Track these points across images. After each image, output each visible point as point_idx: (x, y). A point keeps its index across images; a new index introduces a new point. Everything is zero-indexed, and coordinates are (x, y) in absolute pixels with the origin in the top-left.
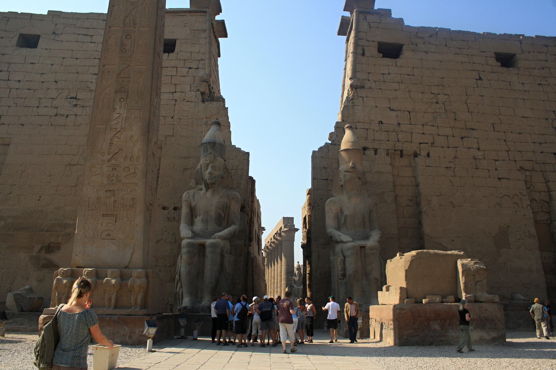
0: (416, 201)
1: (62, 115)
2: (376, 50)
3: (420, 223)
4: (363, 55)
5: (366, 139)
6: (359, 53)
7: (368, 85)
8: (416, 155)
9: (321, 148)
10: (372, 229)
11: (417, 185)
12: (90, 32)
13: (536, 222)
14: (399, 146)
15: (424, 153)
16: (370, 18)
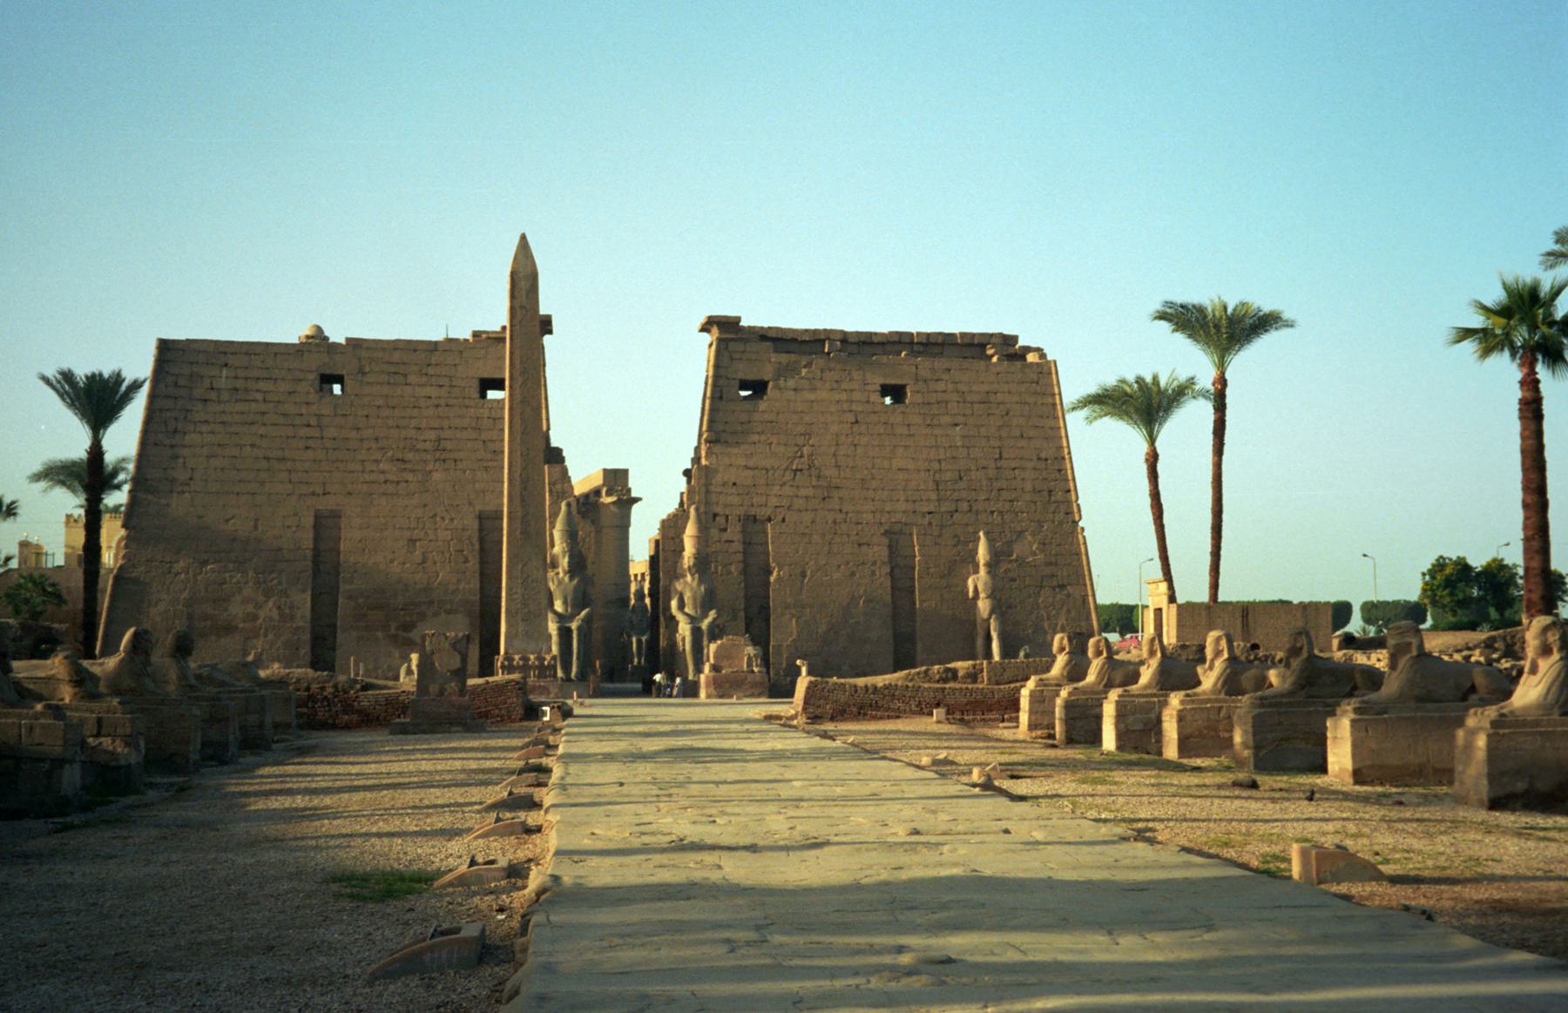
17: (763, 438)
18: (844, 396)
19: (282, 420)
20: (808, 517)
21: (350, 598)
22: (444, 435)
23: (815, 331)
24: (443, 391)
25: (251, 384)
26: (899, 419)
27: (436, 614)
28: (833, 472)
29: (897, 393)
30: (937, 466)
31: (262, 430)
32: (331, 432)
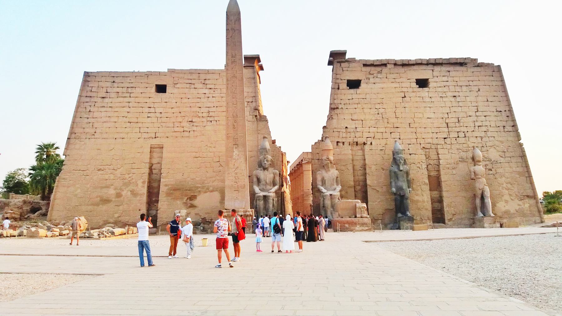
0: (364, 167)
1: (187, 131)
2: (346, 85)
3: (365, 180)
4: (338, 89)
5: (339, 137)
6: (336, 88)
7: (340, 107)
8: (364, 144)
9: (316, 143)
10: (337, 185)
11: (365, 160)
12: (193, 82)
13: (429, 176)
14: (356, 140)
15: (369, 143)
16: (343, 64)
17: (359, 106)
18: (397, 85)
19: (136, 105)
20: (383, 142)
21: (166, 185)
22: (210, 110)
23: (381, 60)
24: (212, 91)
25: (125, 90)
26: (427, 94)
27: (205, 192)
28: (395, 120)
29: (422, 83)
30: (446, 116)
31: (128, 110)
32: (158, 110)
